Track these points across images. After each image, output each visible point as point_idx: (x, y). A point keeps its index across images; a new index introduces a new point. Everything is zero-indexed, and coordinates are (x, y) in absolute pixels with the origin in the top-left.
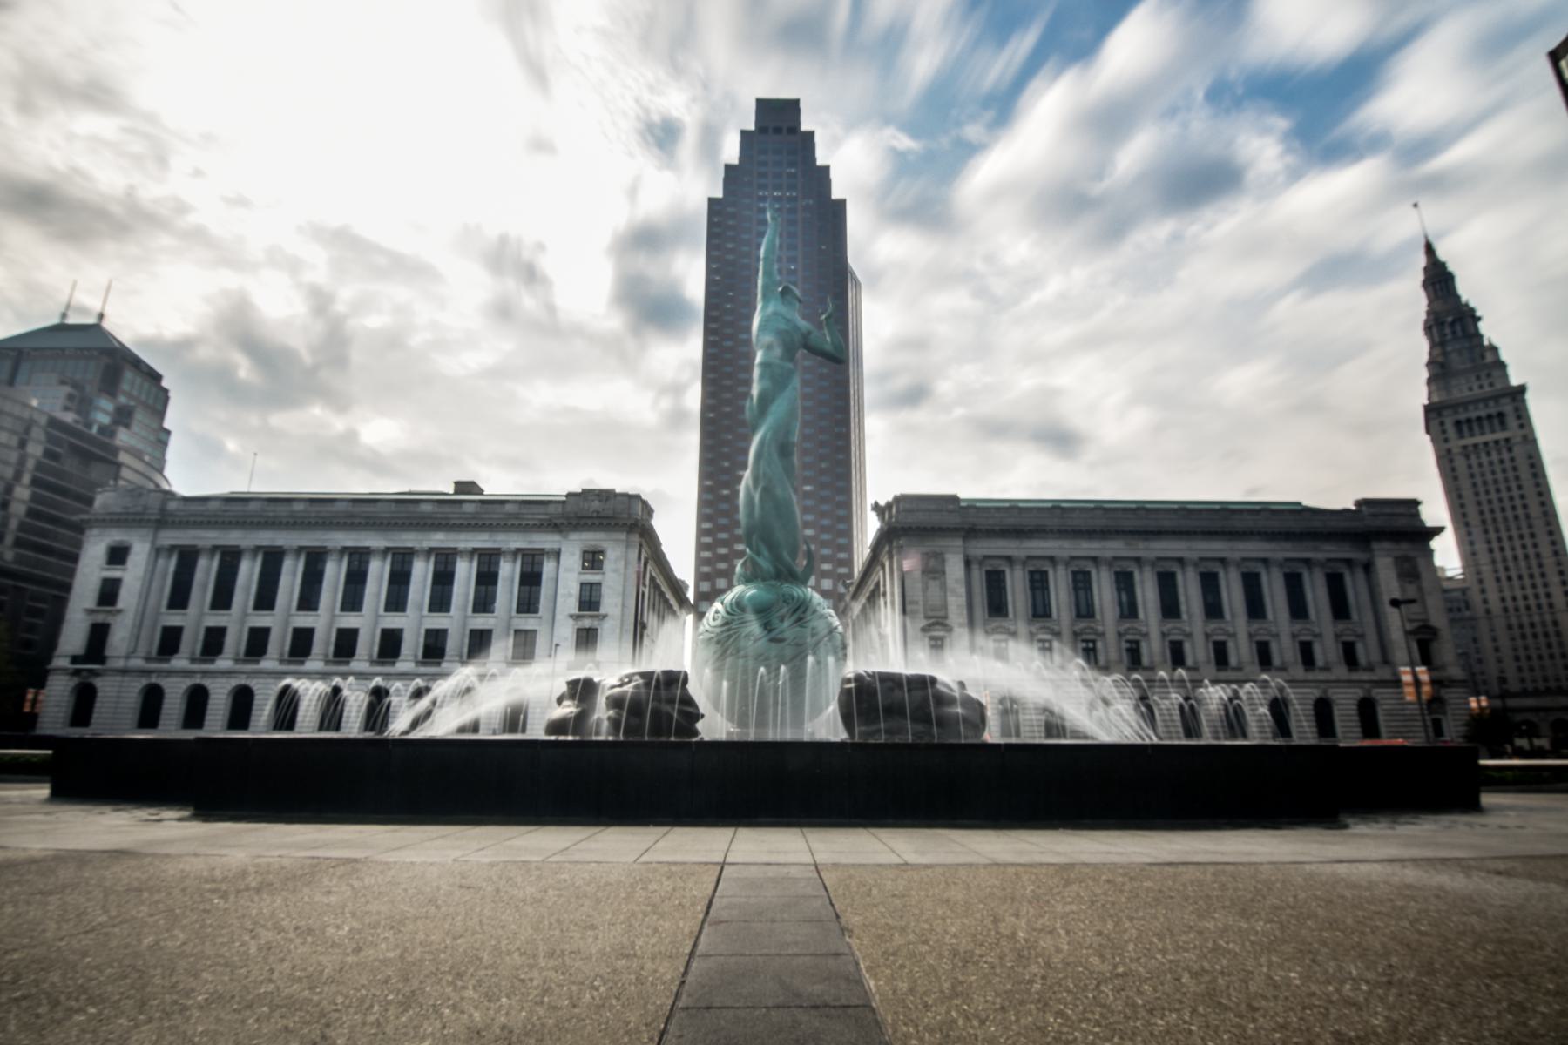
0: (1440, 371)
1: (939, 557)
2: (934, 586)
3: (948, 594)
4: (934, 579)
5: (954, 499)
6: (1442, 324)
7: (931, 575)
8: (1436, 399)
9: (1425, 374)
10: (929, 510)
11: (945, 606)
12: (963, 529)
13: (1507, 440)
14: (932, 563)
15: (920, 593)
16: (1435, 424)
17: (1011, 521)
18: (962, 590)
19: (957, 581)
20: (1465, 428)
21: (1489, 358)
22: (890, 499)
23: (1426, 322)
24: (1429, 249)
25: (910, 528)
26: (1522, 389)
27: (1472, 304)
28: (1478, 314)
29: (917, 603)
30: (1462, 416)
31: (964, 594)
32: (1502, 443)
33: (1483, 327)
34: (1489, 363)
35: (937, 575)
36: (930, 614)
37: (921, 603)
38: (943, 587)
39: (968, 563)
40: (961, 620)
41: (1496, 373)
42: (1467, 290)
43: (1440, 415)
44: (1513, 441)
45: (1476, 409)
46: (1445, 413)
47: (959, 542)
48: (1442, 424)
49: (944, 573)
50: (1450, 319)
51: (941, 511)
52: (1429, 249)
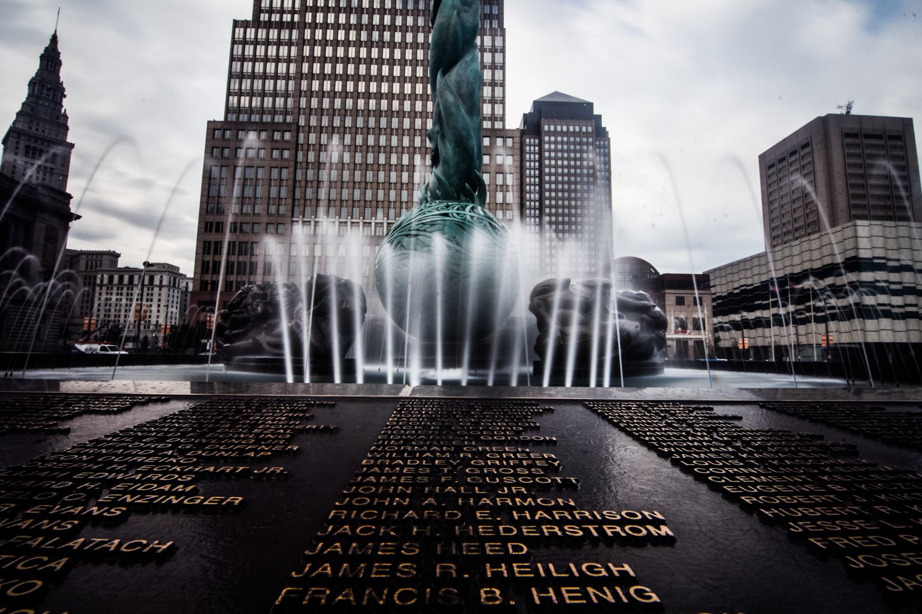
0: (27, 112)
6: (43, 86)
8: (19, 126)
9: (18, 108)
13: (52, 169)
16: (12, 141)
20: (31, 151)
21: (61, 120)
23: (33, 79)
24: (54, 39)
26: (72, 146)
27: (64, 86)
28: (65, 93)
30: (32, 145)
32: (49, 170)
33: (65, 102)
34: (60, 123)
41: (62, 131)
42: (66, 74)
43: (19, 137)
44: (55, 171)
45: (42, 144)
46: (22, 137)
48: (18, 143)
50: (49, 86)
52: (54, 39)
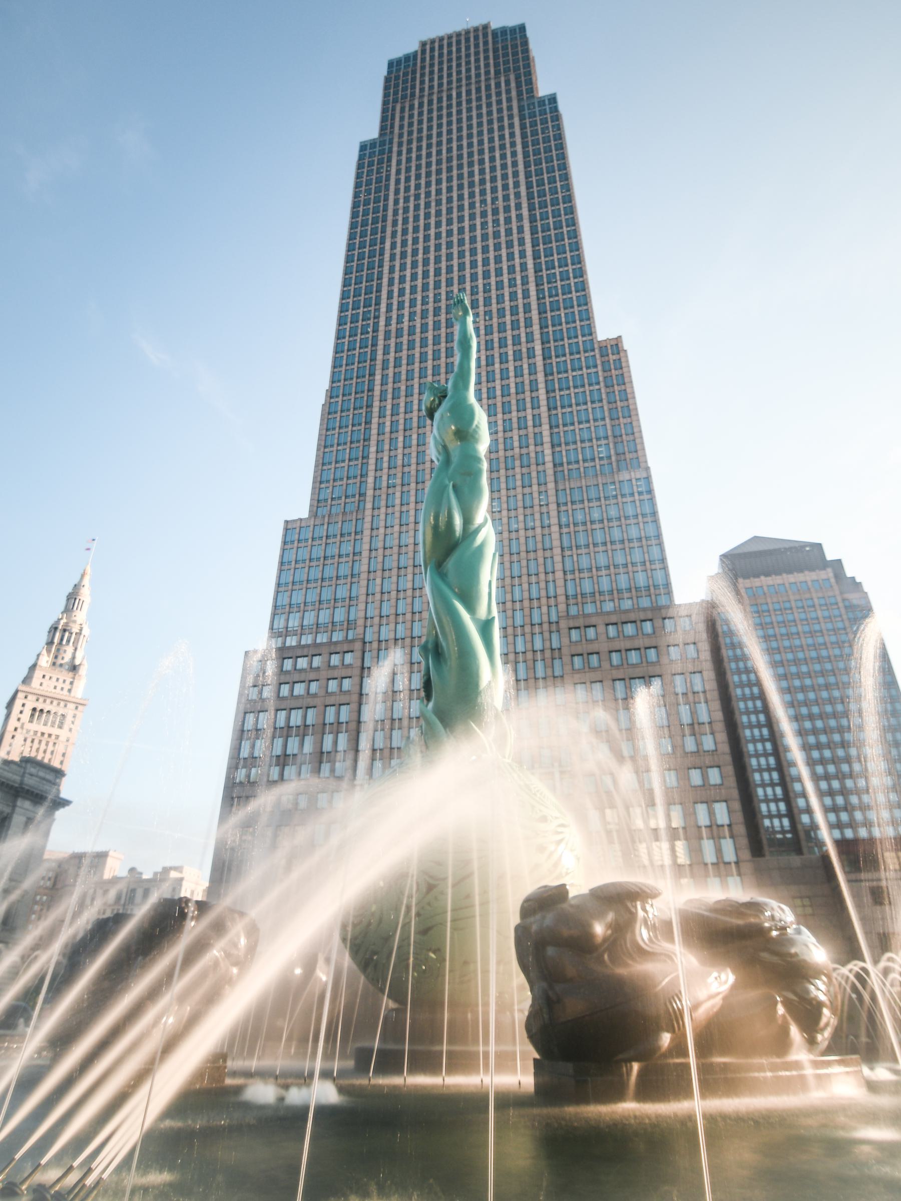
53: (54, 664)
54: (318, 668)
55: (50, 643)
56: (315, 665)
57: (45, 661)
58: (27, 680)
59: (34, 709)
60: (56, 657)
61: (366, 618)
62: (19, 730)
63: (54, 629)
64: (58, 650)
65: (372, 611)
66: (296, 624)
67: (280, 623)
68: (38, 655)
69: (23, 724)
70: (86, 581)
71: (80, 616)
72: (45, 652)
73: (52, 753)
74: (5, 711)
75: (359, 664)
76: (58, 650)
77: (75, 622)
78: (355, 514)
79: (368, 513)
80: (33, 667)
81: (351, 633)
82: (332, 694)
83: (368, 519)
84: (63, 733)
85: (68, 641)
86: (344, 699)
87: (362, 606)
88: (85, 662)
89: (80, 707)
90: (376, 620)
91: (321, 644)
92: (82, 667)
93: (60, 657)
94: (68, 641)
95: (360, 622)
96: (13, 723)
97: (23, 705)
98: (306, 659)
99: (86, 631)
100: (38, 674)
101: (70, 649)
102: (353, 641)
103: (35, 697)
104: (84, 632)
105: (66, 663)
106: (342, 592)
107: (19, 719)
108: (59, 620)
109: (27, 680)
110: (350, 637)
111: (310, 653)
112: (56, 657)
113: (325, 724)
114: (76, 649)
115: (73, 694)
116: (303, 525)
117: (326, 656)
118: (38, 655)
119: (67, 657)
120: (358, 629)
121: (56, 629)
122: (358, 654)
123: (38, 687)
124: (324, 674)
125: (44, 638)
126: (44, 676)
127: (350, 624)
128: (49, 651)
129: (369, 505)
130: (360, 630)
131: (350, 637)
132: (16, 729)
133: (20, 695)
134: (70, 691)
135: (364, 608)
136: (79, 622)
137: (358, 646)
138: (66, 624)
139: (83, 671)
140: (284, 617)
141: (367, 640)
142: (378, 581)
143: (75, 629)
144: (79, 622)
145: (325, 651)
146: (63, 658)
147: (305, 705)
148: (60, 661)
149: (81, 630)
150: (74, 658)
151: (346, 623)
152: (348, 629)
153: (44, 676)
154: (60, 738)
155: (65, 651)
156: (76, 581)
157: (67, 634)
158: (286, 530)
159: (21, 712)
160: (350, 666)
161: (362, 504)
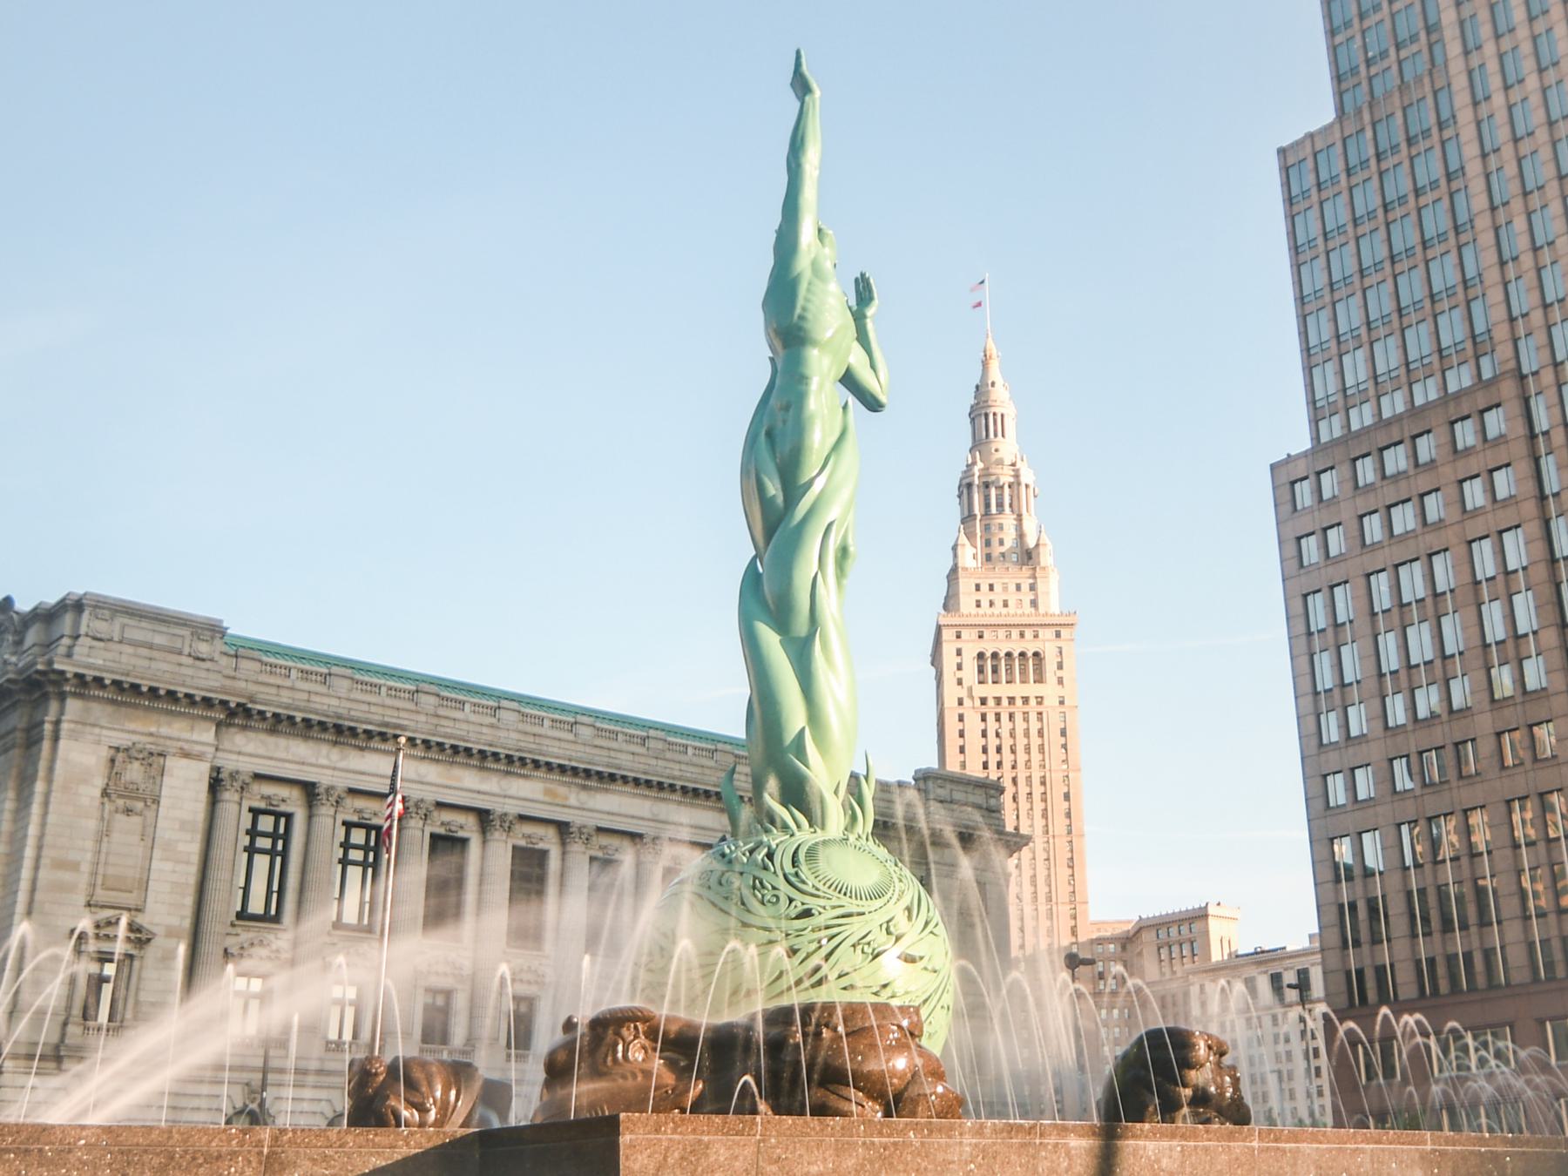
1: (153, 758)
2: (126, 829)
3: (157, 853)
4: (128, 811)
5: (214, 630)
7: (120, 802)
10: (150, 646)
11: (144, 885)
12: (224, 703)
14: (134, 772)
15: (90, 844)
17: (329, 702)
18: (192, 848)
19: (184, 826)
22: (52, 599)
25: (99, 681)
29: (74, 866)
31: (195, 859)
35: (139, 805)
36: (101, 896)
37: (86, 868)
38: (149, 838)
39: (216, 785)
40: (174, 921)
47: (205, 734)
49: (157, 801)
51: (180, 653)
53: (988, 558)
54: (1432, 461)
55: (968, 519)
56: (1424, 457)
57: (969, 556)
58: (950, 602)
59: (981, 656)
60: (988, 543)
61: (1512, 320)
62: (967, 702)
63: (966, 487)
64: (987, 528)
65: (1524, 299)
66: (1362, 376)
67: (1327, 383)
68: (955, 548)
69: (970, 689)
70: (995, 374)
71: (1007, 447)
72: (963, 539)
73: (1041, 733)
74: (933, 670)
75: (1520, 429)
76: (987, 528)
77: (1000, 462)
78: (1427, 80)
79: (1457, 66)
80: (953, 574)
81: (1485, 363)
82: (1477, 512)
83: (1460, 82)
84: (1049, 690)
85: (1000, 505)
86: (1505, 518)
87: (1496, 295)
88: (1045, 539)
89: (1064, 632)
90: (1537, 317)
91: (1428, 406)
92: (1041, 549)
93: (995, 542)
94: (1000, 505)
95: (1501, 333)
96: (951, 692)
97: (959, 652)
98: (1400, 448)
99: (1027, 476)
100: (965, 585)
101: (1008, 520)
102: (1495, 380)
103: (974, 633)
104: (1024, 480)
105: (1012, 551)
106: (1445, 274)
107: (960, 682)
108: (970, 467)
109: (950, 602)
110: (1487, 374)
111: (1407, 435)
112: (988, 543)
113: (1477, 583)
114: (1019, 518)
115: (1042, 610)
116: (1319, 145)
117: (1441, 433)
118: (955, 548)
119: (1010, 541)
120: (1499, 348)
121: (970, 486)
122: (1515, 407)
123: (974, 610)
124: (1448, 473)
125: (955, 511)
126: (978, 588)
127: (1478, 345)
128: (970, 536)
129: (1454, 49)
130: (1504, 351)
131: (1487, 374)
132: (960, 702)
133: (947, 635)
134: (1034, 603)
135: (1500, 296)
136: (1008, 461)
137: (1508, 388)
138: (986, 472)
139: (1046, 558)
140: (1361, 355)
141: (1525, 370)
142: (1520, 224)
143: (1006, 478)
144: (1008, 461)
145: (1437, 419)
146: (1001, 542)
147: (1423, 553)
148: (997, 550)
149: (1017, 476)
150: (1021, 536)
151: (1469, 345)
152: (1477, 358)
153: (978, 588)
154: (1046, 702)
155: (1001, 527)
156: (977, 381)
157: (993, 492)
158: (1286, 170)
159: (959, 667)
160: (1501, 439)
161: (1437, 49)
